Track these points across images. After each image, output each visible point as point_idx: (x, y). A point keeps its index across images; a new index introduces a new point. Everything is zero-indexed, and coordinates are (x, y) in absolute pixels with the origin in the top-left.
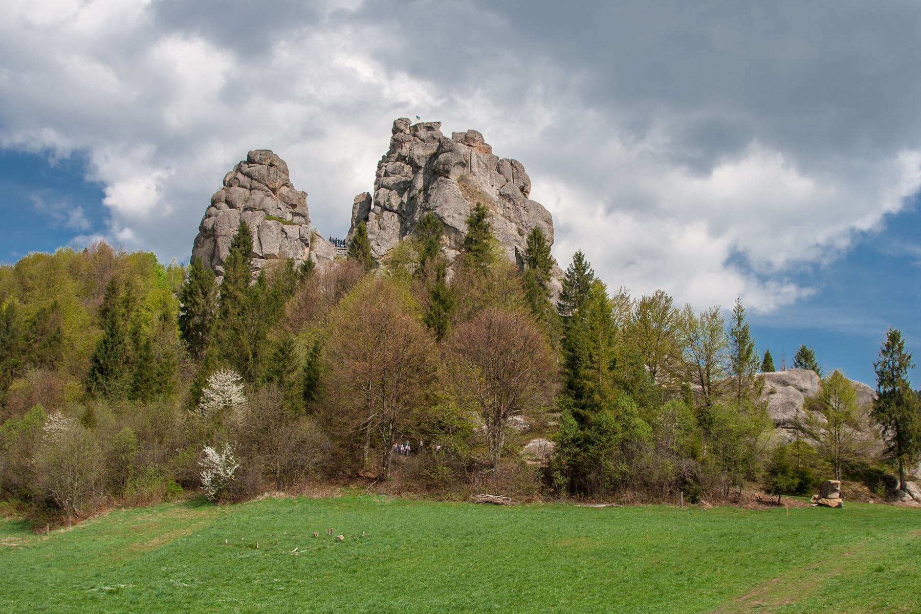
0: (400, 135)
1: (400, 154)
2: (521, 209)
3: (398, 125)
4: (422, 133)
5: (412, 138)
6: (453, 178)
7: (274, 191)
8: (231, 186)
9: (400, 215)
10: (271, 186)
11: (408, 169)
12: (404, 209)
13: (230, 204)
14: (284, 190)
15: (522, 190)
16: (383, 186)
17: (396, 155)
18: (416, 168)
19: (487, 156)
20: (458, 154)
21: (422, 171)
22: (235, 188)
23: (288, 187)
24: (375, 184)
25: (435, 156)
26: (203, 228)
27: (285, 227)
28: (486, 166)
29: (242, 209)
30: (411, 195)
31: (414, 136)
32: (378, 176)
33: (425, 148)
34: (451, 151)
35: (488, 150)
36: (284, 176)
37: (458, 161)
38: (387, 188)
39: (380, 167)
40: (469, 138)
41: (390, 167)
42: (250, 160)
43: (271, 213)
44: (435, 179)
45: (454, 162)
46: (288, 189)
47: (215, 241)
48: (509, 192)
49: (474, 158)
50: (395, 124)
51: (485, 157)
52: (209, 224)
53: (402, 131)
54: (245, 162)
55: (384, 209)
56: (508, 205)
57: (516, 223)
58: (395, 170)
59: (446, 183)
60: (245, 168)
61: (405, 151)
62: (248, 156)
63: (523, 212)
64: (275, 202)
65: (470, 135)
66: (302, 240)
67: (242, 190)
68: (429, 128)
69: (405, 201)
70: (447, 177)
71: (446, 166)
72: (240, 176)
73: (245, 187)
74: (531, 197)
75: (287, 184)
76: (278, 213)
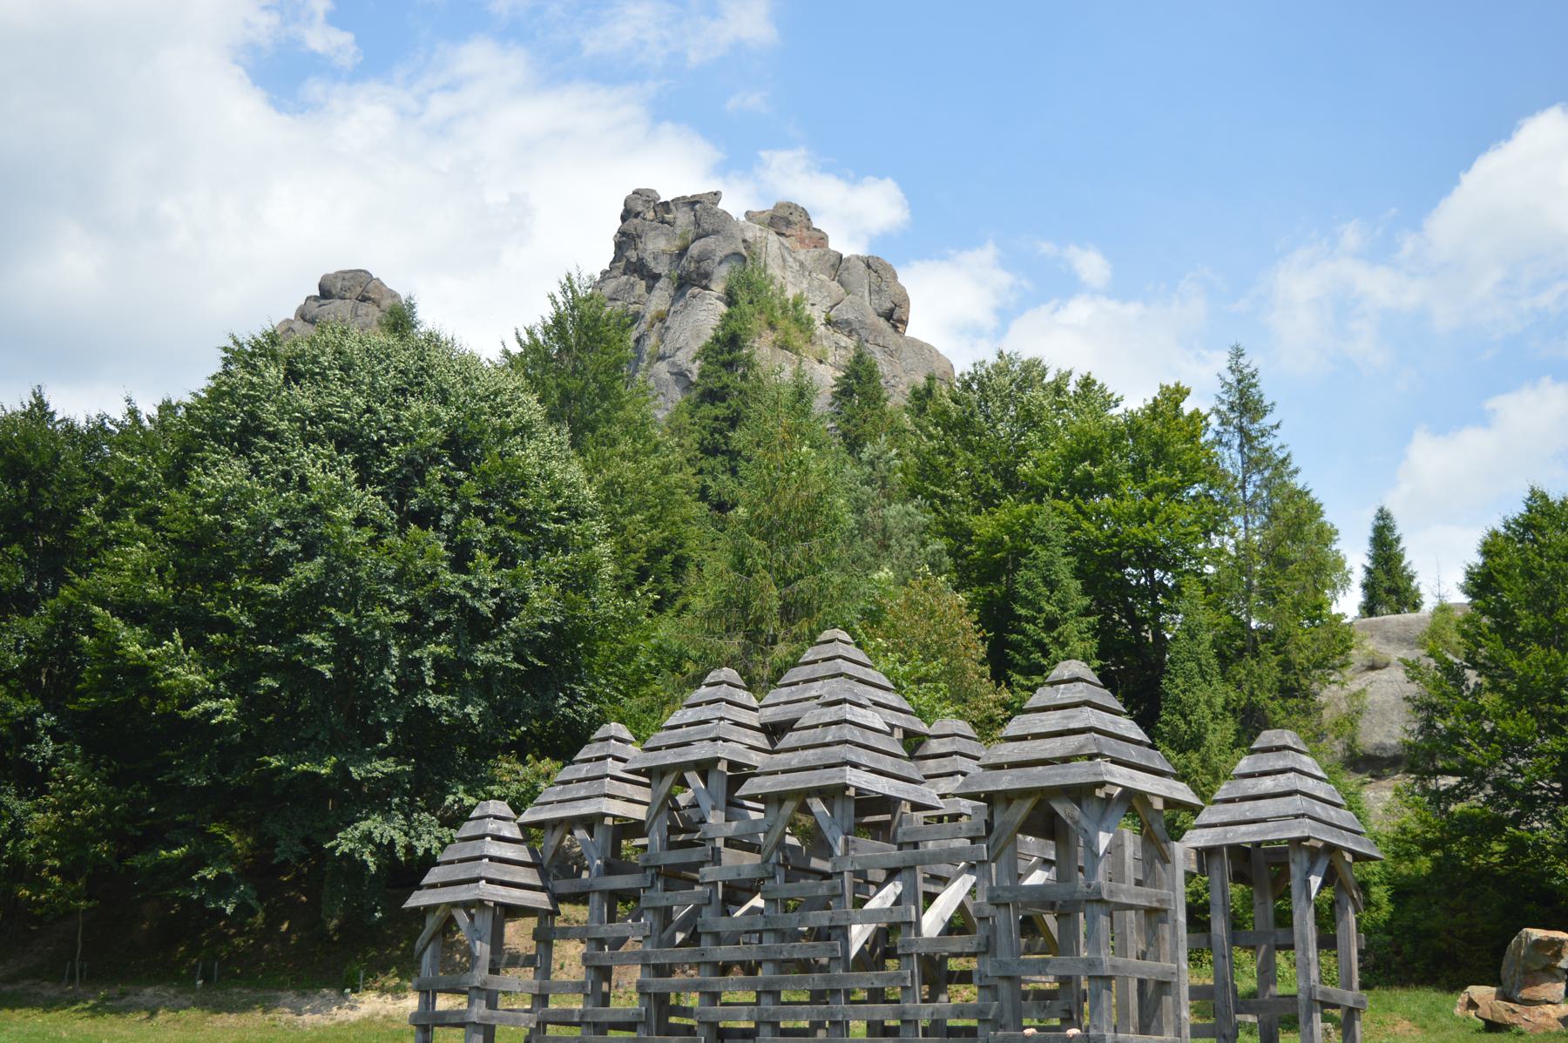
15: (888, 316)
17: (622, 264)
34: (716, 232)
45: (720, 254)
48: (851, 316)
51: (806, 255)
59: (703, 299)
65: (781, 213)
70: (706, 288)
71: (704, 265)
74: (912, 331)
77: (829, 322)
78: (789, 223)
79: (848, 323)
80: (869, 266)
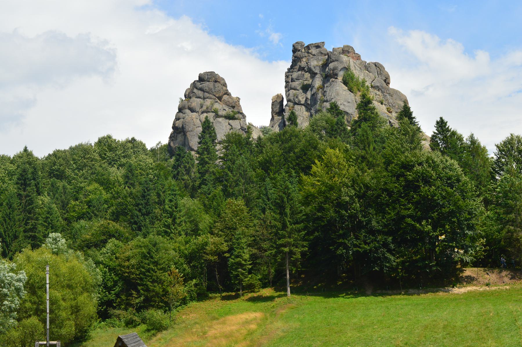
0: (298, 54)
1: (300, 66)
2: (387, 95)
3: (297, 47)
4: (313, 51)
5: (306, 54)
6: (340, 79)
7: (220, 98)
8: (190, 98)
9: (306, 107)
10: (217, 95)
11: (307, 75)
12: (309, 102)
13: (192, 110)
14: (225, 97)
15: (385, 81)
16: (292, 89)
17: (297, 67)
18: (313, 75)
19: (358, 62)
20: (342, 62)
22: (194, 99)
23: (228, 95)
24: (286, 87)
25: (325, 65)
26: (174, 127)
27: (231, 121)
28: (360, 68)
29: (200, 113)
30: (313, 93)
31: (308, 53)
32: (287, 82)
33: (318, 60)
34: (337, 60)
35: (358, 57)
36: (224, 88)
37: (342, 67)
38: (295, 89)
39: (287, 77)
40: (347, 51)
41: (295, 75)
42: (201, 79)
43: (220, 113)
44: (328, 81)
45: (340, 68)
46: (228, 96)
47: (185, 135)
48: (378, 85)
49: (352, 64)
50: (293, 46)
52: (179, 124)
53: (299, 51)
54: (197, 81)
55: (295, 103)
56: (378, 93)
57: (385, 105)
58: (298, 77)
59: (336, 82)
60: (199, 85)
61: (303, 64)
62: (199, 77)
63: (388, 97)
64: (221, 106)
65: (346, 49)
66: (242, 129)
67: (198, 100)
68: (317, 46)
69: (309, 97)
70: (336, 78)
71: (335, 71)
72: (195, 90)
74: (391, 86)
75: (227, 93)
76: (224, 113)
78: (349, 52)
79: (378, 87)
80: (376, 66)
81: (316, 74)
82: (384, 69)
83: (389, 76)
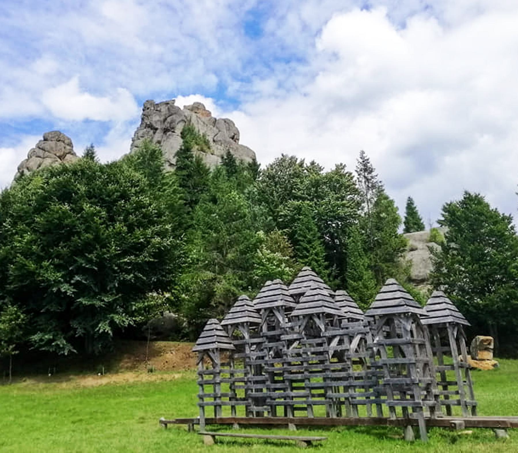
10: (58, 155)
15: (233, 138)
17: (144, 125)
21: (158, 131)
34: (175, 113)
36: (68, 147)
37: (180, 119)
46: (71, 156)
51: (205, 119)
62: (44, 137)
65: (196, 106)
70: (174, 132)
73: (40, 157)
74: (240, 142)
77: (214, 141)
78: (198, 108)
79: (220, 141)
80: (225, 122)
81: (156, 129)
82: (234, 125)
83: (238, 132)
